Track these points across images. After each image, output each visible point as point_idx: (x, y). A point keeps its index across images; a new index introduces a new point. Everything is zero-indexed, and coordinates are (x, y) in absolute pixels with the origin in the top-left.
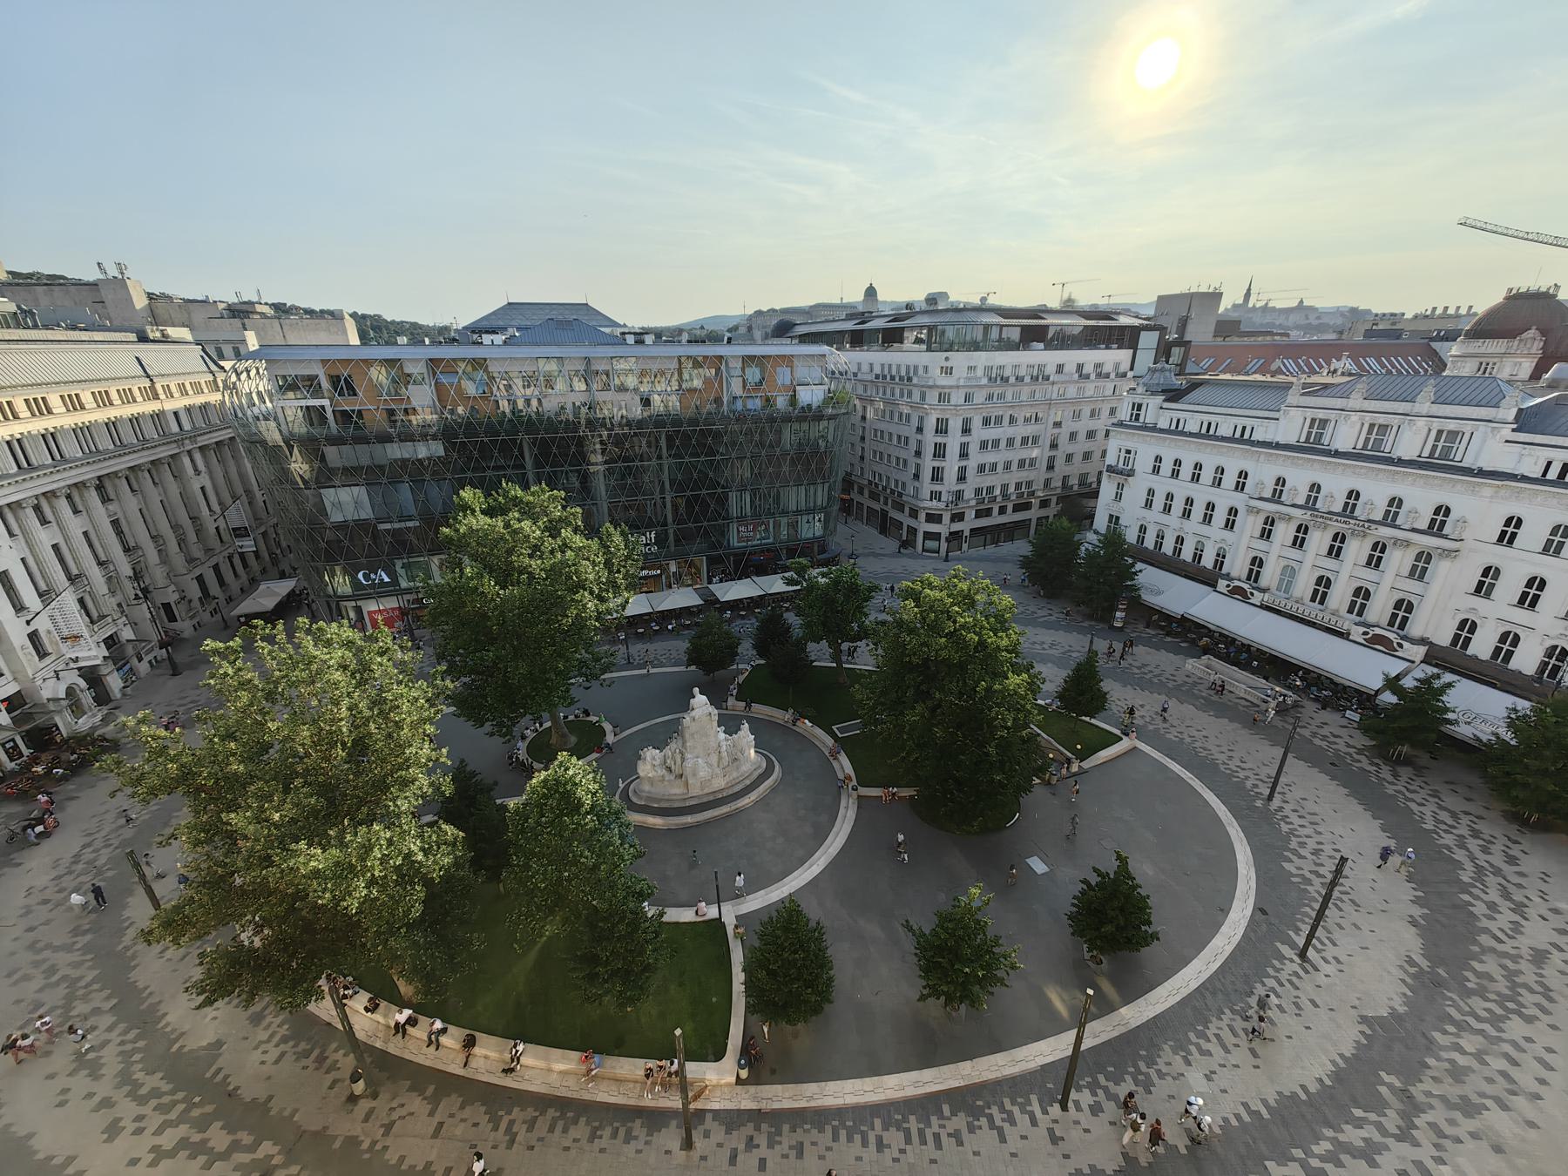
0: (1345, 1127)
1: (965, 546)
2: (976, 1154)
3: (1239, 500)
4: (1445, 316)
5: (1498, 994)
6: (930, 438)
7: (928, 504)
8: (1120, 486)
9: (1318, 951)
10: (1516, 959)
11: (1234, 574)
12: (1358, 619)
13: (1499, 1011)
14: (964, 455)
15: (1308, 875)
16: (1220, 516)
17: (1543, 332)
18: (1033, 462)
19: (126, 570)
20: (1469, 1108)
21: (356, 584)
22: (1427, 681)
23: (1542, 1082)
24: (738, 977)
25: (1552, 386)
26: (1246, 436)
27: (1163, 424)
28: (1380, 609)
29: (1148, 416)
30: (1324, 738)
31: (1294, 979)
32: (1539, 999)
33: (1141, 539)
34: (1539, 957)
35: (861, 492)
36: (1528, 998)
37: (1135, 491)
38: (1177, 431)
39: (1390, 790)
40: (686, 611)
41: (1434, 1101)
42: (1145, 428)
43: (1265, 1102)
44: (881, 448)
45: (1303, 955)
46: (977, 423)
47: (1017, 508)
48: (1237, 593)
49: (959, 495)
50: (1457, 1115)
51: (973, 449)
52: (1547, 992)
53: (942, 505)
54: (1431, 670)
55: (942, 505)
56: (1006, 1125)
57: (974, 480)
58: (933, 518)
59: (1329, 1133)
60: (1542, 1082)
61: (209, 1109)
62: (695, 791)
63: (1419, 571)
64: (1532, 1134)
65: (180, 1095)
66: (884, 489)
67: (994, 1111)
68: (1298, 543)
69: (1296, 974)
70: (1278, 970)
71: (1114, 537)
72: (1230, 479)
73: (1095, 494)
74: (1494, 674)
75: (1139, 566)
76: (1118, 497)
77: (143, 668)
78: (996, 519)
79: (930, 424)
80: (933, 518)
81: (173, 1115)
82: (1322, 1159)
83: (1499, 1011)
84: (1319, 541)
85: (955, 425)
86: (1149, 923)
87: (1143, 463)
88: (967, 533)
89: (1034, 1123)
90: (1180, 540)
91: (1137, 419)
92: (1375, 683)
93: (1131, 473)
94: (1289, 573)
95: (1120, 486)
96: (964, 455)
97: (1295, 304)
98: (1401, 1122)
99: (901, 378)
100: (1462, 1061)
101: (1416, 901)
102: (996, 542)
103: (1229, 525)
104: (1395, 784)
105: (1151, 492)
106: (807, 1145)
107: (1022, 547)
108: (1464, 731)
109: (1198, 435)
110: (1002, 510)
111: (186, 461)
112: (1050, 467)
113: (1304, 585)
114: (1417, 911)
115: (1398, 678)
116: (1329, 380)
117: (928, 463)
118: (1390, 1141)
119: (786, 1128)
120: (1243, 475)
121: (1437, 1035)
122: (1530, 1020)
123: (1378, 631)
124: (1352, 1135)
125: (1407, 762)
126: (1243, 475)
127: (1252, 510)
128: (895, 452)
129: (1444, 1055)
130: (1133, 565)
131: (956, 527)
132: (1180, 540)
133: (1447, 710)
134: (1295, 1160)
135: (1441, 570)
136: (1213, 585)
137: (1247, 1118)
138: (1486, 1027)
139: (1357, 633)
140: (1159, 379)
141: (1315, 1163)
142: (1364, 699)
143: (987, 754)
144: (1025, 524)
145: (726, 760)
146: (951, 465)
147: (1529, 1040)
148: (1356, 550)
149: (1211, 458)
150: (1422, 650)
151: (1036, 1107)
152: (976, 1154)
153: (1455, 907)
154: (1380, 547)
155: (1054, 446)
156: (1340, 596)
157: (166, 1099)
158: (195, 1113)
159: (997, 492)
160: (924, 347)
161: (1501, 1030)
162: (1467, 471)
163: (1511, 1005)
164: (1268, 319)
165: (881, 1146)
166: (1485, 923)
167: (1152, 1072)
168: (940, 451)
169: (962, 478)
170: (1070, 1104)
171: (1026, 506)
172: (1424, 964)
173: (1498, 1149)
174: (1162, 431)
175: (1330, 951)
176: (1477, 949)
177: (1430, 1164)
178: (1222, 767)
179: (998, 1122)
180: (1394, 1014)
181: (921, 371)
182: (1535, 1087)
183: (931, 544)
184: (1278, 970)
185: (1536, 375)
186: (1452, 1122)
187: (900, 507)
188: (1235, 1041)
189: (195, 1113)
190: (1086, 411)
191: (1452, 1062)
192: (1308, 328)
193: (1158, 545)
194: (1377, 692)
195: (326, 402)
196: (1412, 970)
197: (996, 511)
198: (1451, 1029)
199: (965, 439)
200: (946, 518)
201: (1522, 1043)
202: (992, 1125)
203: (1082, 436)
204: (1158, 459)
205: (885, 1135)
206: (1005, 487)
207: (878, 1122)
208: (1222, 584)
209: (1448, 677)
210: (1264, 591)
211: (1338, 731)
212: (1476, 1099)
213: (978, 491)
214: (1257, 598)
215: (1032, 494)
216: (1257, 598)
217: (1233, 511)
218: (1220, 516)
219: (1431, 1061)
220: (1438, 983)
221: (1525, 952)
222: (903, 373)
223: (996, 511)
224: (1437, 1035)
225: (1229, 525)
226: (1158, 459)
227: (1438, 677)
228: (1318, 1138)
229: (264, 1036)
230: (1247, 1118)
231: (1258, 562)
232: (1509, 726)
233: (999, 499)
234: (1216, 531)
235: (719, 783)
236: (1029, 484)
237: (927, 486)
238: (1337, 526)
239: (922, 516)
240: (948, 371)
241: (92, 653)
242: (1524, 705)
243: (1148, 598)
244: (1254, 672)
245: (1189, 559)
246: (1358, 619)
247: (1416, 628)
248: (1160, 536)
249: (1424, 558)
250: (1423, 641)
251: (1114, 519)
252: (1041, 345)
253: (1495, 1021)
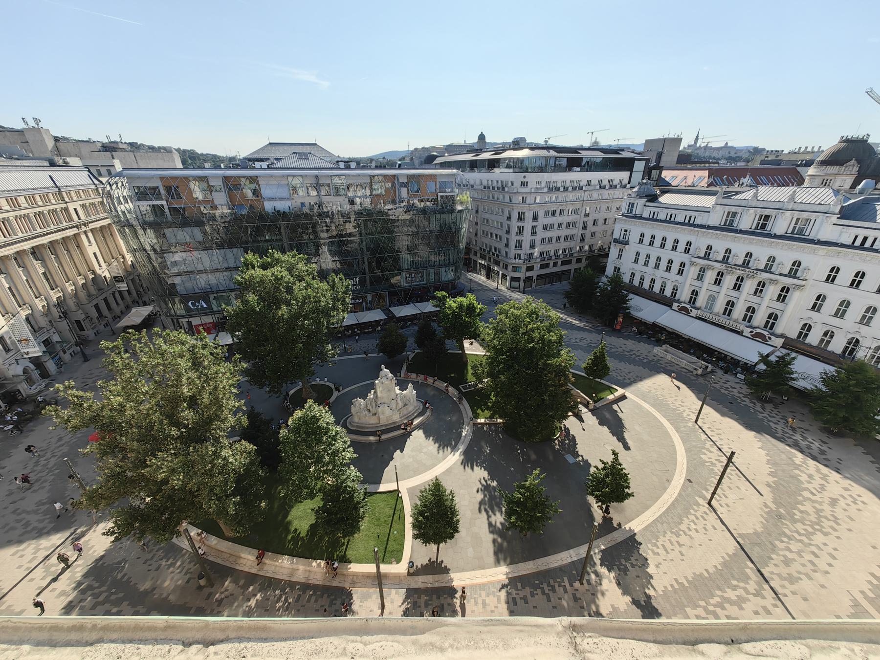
0: (727, 590)
1: (534, 285)
2: (534, 607)
3: (685, 258)
4: (806, 152)
5: (811, 521)
6: (515, 224)
7: (514, 261)
8: (621, 251)
9: (718, 501)
10: (821, 503)
11: (682, 299)
12: (748, 324)
13: (810, 530)
14: (534, 233)
15: (714, 462)
16: (675, 267)
17: (859, 161)
18: (572, 237)
20: (792, 580)
21: (187, 309)
22: (782, 358)
23: (830, 565)
24: (409, 520)
25: (861, 193)
26: (691, 222)
27: (646, 215)
28: (760, 319)
29: (637, 211)
30: (727, 389)
31: (704, 515)
32: (832, 524)
33: (632, 280)
34: (833, 502)
35: (476, 254)
36: (826, 523)
37: (629, 252)
38: (653, 219)
39: (760, 416)
40: (377, 322)
41: (774, 576)
42: (636, 217)
43: (686, 578)
44: (487, 229)
45: (709, 503)
46: (541, 214)
47: (563, 263)
48: (684, 310)
49: (531, 256)
50: (786, 583)
51: (539, 229)
52: (836, 520)
53: (521, 262)
54: (784, 351)
56: (551, 593)
58: (515, 269)
59: (718, 593)
60: (830, 565)
61: (121, 595)
62: (383, 422)
63: (782, 297)
64: (823, 591)
65: (104, 588)
66: (489, 252)
67: (545, 586)
68: (718, 282)
69: (705, 513)
70: (696, 511)
71: (616, 279)
72: (681, 247)
73: (607, 255)
74: (819, 354)
75: (631, 296)
76: (620, 257)
78: (551, 270)
79: (515, 216)
80: (515, 269)
81: (101, 599)
82: (715, 606)
83: (810, 530)
84: (729, 280)
85: (529, 216)
86: (628, 487)
87: (634, 238)
88: (535, 277)
89: (566, 591)
90: (653, 281)
91: (631, 213)
92: (755, 359)
93: (627, 243)
94: (712, 299)
95: (621, 251)
96: (534, 233)
97: (723, 145)
98: (756, 587)
99: (499, 189)
100: (790, 555)
101: (771, 474)
102: (551, 282)
103: (680, 272)
104: (764, 413)
105: (638, 254)
106: (446, 606)
107: (564, 285)
108: (801, 384)
109: (665, 221)
110: (555, 264)
111: (83, 237)
112: (582, 240)
113: (720, 306)
114: (771, 480)
115: (768, 356)
116: (739, 189)
117: (514, 238)
118: (750, 597)
119: (434, 597)
120: (689, 244)
121: (777, 543)
122: (826, 534)
123: (758, 330)
124: (731, 594)
125: (770, 401)
126: (689, 244)
127: (692, 264)
128: (495, 231)
129: (781, 553)
130: (626, 296)
131: (529, 274)
132: (653, 281)
133: (792, 373)
134: (700, 606)
135: (795, 297)
136: (670, 306)
137: (676, 586)
138: (804, 538)
139: (747, 331)
140: (645, 189)
141: (711, 608)
142: (748, 368)
143: (543, 400)
145: (400, 404)
146: (527, 237)
147: (825, 544)
148: (749, 286)
149: (671, 233)
150: (782, 341)
151: (566, 583)
152: (534, 607)
153: (792, 477)
154: (762, 285)
155: (585, 227)
156: (739, 311)
157: (96, 591)
158: (113, 597)
159: (552, 253)
160: (511, 170)
161: (810, 540)
162: (812, 241)
163: (817, 527)
164: (707, 154)
165: (484, 604)
166: (806, 485)
167: (629, 565)
168: (521, 230)
169: (532, 247)
170: (585, 582)
171: (568, 262)
172: (773, 507)
173: (805, 599)
174: (645, 219)
175: (724, 501)
176: (801, 498)
177: (770, 608)
178: (671, 405)
179: (547, 591)
180: (756, 533)
181: (510, 184)
182: (828, 568)
184: (696, 511)
185: (853, 187)
186: (783, 587)
187: (497, 263)
188: (672, 547)
189: (113, 597)
190: (604, 207)
191: (784, 556)
192: (730, 159)
193: (641, 284)
194: (756, 364)
196: (767, 510)
197: (551, 265)
198: (785, 539)
199: (535, 224)
200: (524, 269)
201: (822, 546)
202: (543, 593)
203: (601, 222)
204: (642, 235)
205: (487, 599)
206: (556, 251)
207: (483, 593)
208: (675, 305)
209: (793, 355)
210: (697, 309)
211: (735, 385)
212: (796, 575)
213: (541, 254)
214: (694, 313)
215: (572, 255)
216: (694, 313)
217: (683, 265)
218: (675, 267)
219: (773, 556)
220: (780, 517)
221: (827, 500)
222: (499, 185)
223: (551, 265)
224: (777, 543)
225: (680, 272)
226: (642, 235)
227: (788, 354)
228: (713, 596)
229: (149, 556)
230: (676, 586)
231: (695, 293)
232: (824, 381)
233: (553, 258)
234: (673, 276)
235: (396, 418)
236: (571, 249)
237: (513, 251)
238: (739, 272)
239: (510, 268)
240: (524, 184)
242: (831, 369)
243: (634, 313)
244: (690, 354)
245: (658, 292)
246: (748, 324)
247: (779, 329)
248: (642, 279)
249: (785, 290)
250: (782, 336)
251: (617, 269)
252: (578, 169)
253: (809, 535)
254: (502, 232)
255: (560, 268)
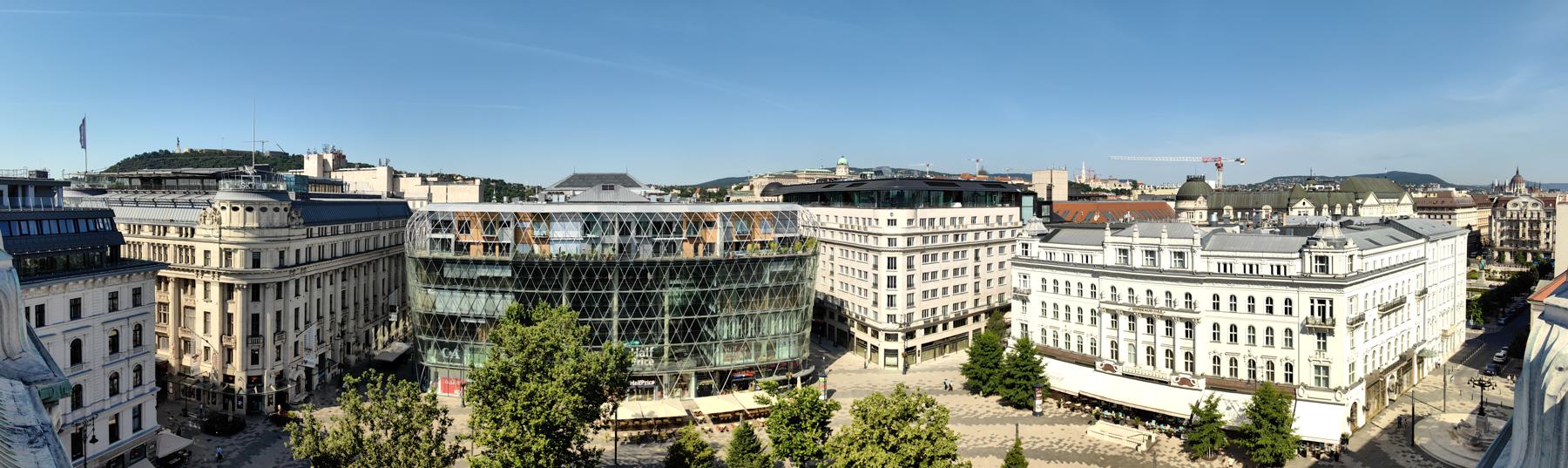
19: (339, 320)
55: (896, 327)
57: (921, 305)
58: (890, 337)
77: (329, 376)
80: (890, 337)
88: (919, 348)
107: (962, 356)
131: (910, 343)
144: (964, 336)
169: (910, 304)
183: (891, 360)
195: (451, 236)
213: (925, 313)
236: (963, 303)
239: (882, 335)
240: (892, 222)
241: (313, 361)
254: (868, 285)
255: (952, 331)
